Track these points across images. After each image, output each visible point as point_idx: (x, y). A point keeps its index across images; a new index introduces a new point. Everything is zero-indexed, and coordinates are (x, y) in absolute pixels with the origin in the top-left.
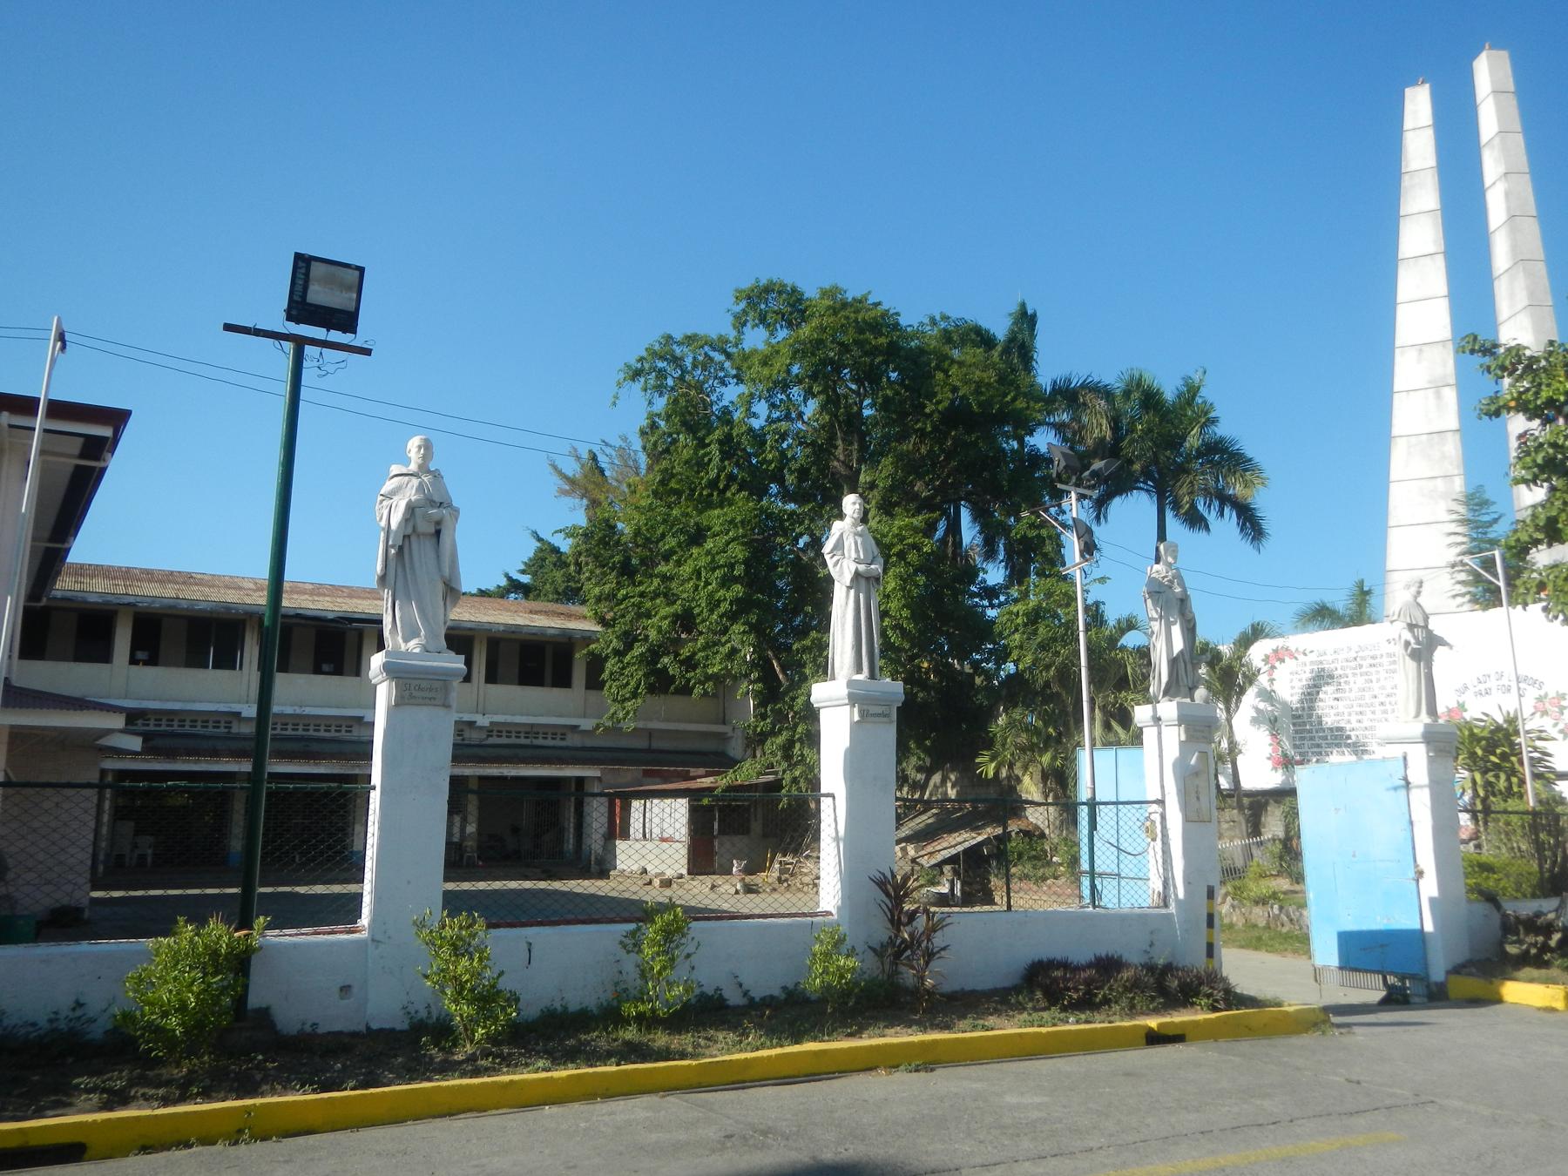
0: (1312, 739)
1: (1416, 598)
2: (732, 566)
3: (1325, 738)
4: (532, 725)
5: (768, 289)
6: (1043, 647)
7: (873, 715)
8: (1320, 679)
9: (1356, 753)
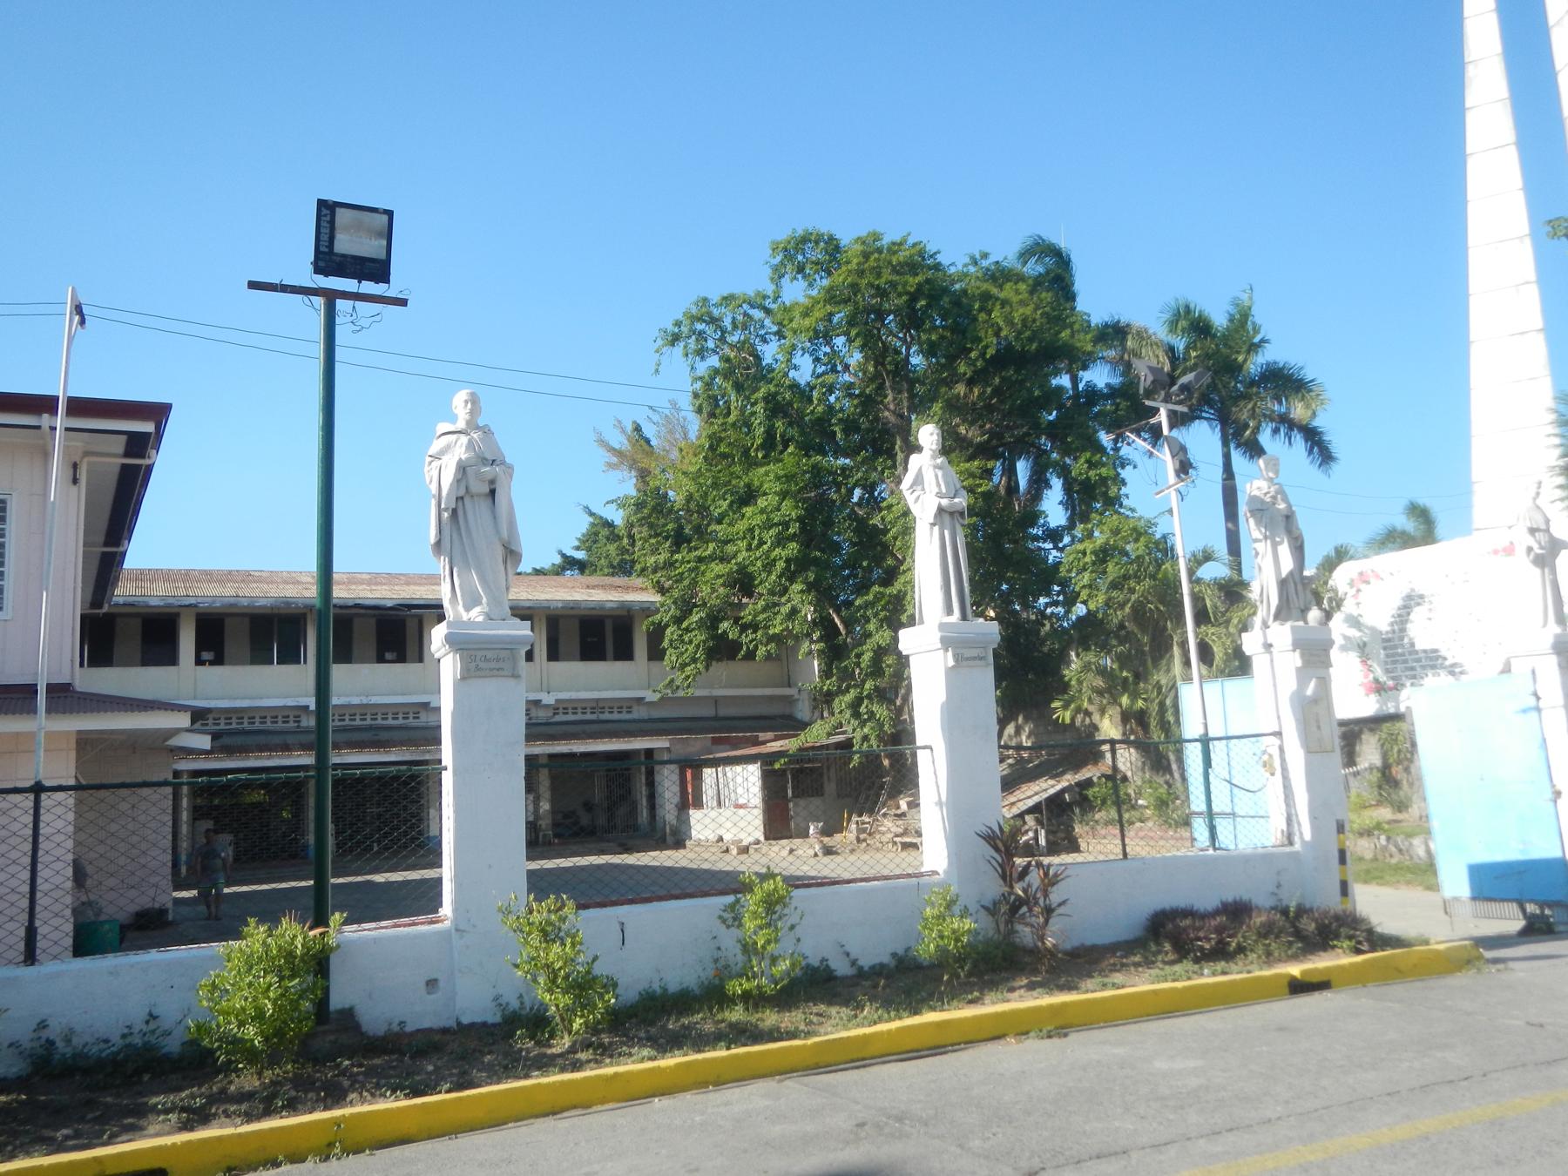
0: (1405, 662)
1: (1535, 499)
2: (786, 525)
3: (1419, 660)
4: (598, 700)
5: (805, 239)
6: (1114, 585)
7: (967, 659)
8: (1411, 601)
9: (1452, 673)
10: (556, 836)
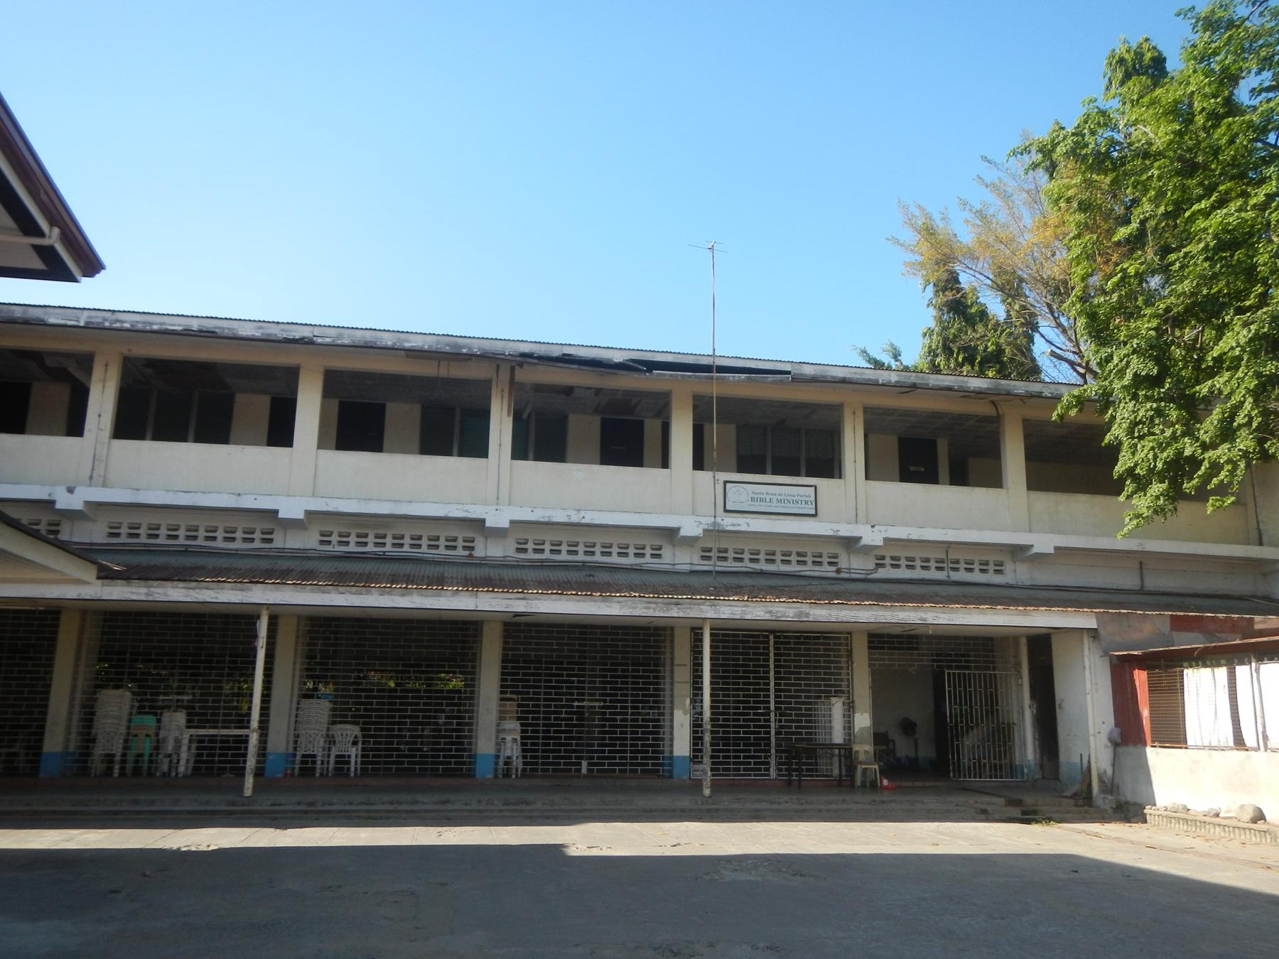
4: (948, 545)
10: (883, 773)
